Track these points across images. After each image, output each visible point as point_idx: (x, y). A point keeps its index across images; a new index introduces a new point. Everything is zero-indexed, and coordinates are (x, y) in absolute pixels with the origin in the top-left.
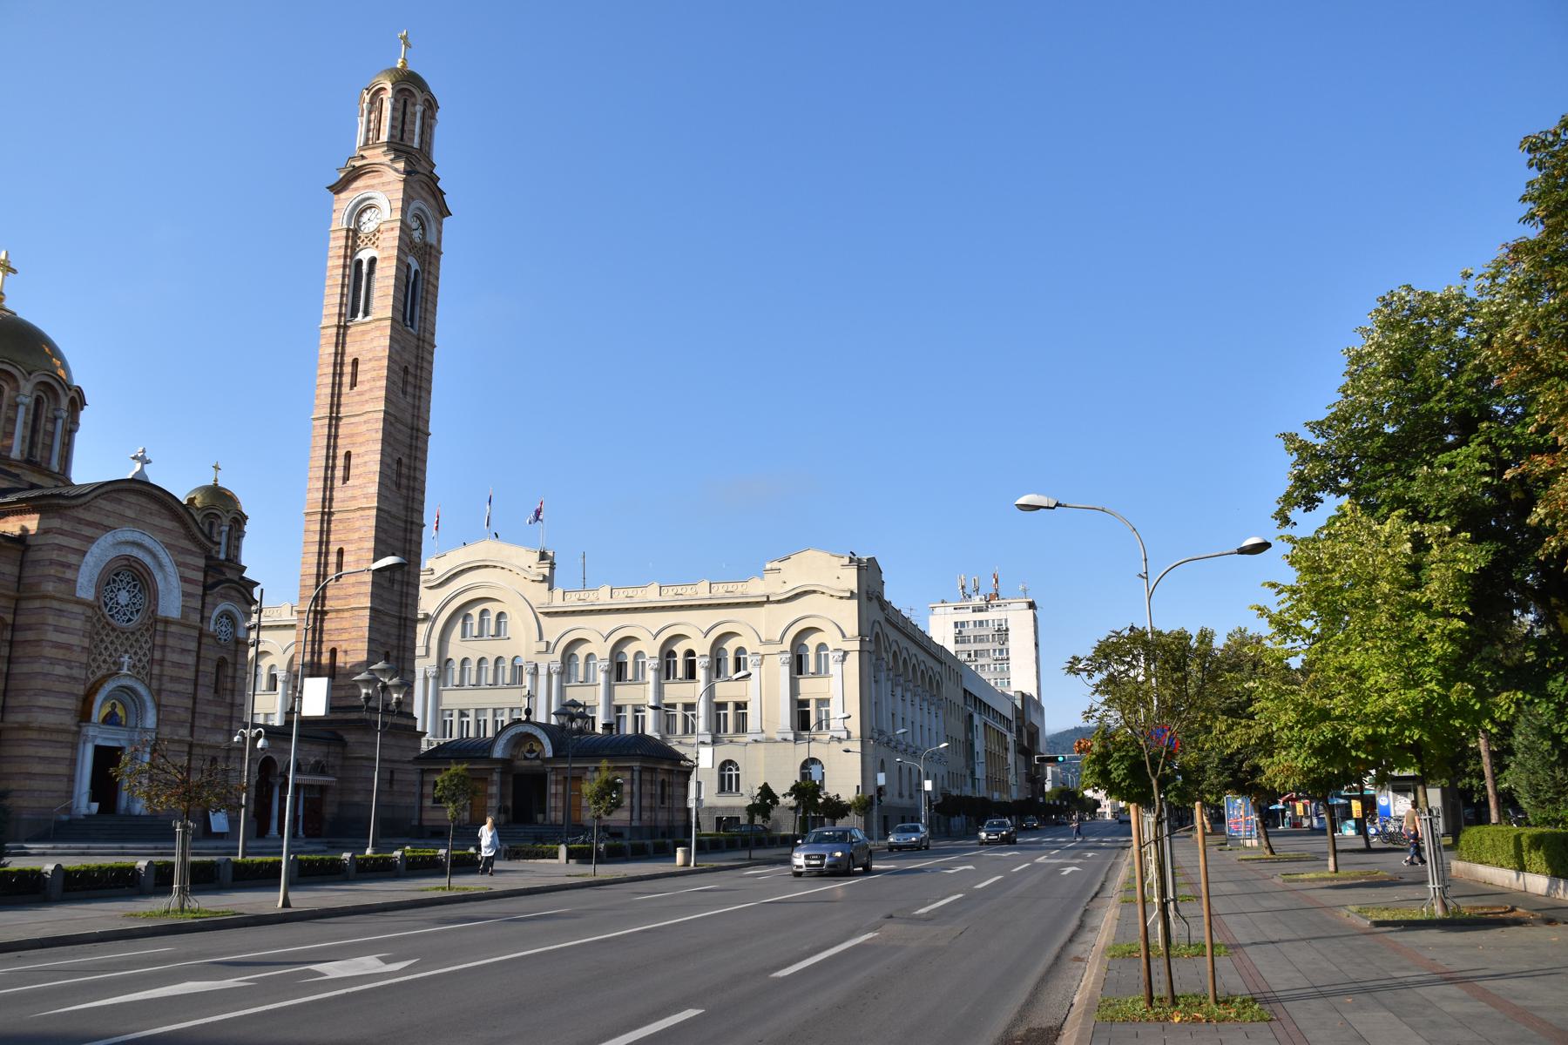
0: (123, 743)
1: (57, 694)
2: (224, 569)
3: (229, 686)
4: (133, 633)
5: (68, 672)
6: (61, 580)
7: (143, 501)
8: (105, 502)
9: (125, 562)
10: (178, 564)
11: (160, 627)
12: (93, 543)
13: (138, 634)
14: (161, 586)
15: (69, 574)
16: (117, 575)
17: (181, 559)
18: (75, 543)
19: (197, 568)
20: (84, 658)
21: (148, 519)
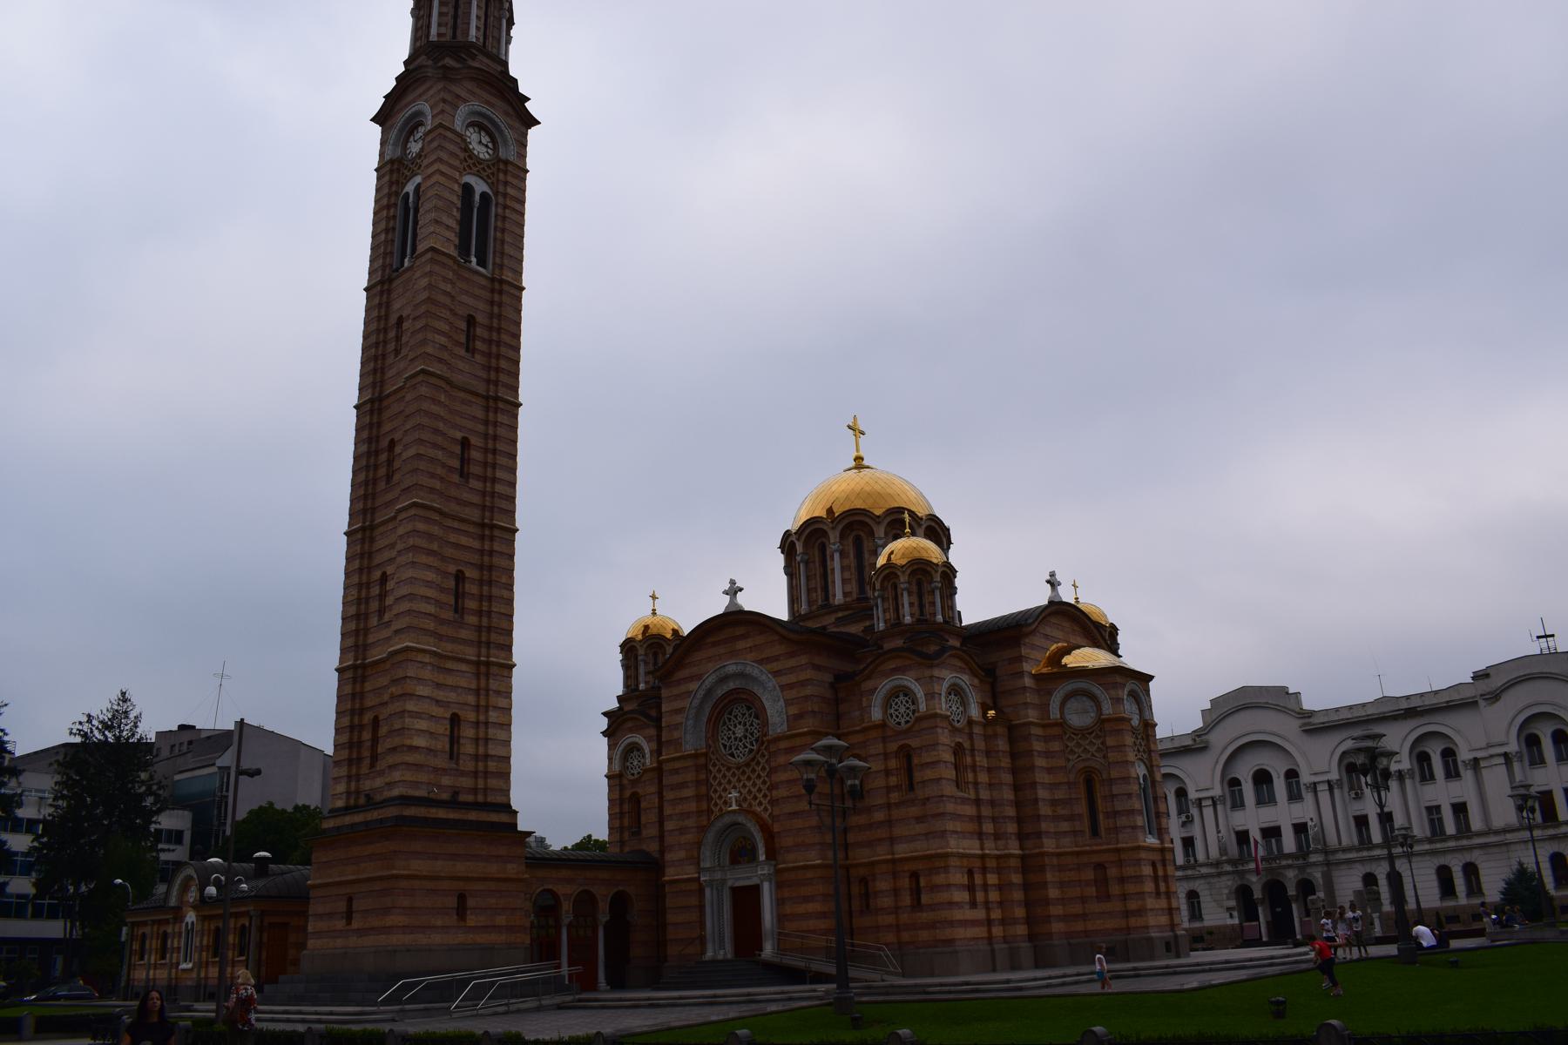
0: (755, 881)
4: (748, 765)
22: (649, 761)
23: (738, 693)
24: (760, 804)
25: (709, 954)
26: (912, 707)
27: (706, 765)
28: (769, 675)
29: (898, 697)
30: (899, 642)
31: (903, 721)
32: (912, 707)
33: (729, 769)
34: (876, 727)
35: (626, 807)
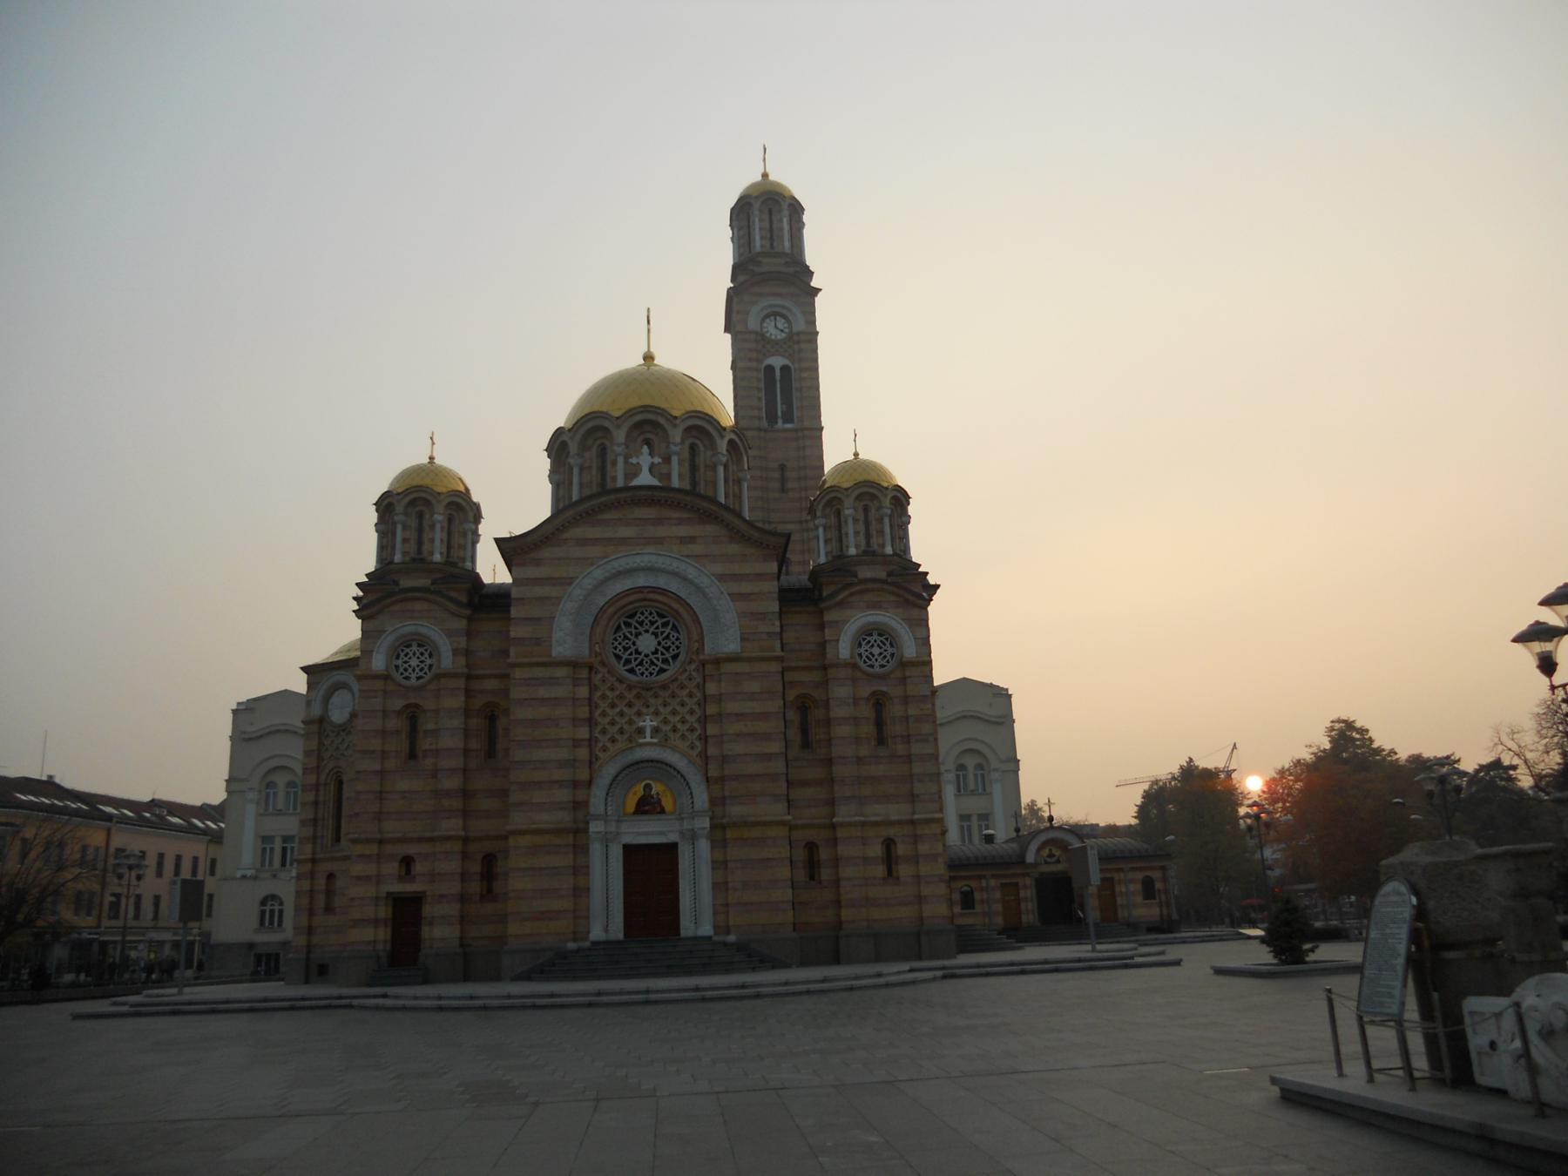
0: (672, 837)
4: (664, 687)
11: (709, 669)
12: (570, 584)
16: (632, 616)
19: (760, 577)
20: (583, 733)
21: (661, 531)
22: (447, 661)
23: (649, 592)
24: (683, 737)
25: (597, 933)
26: (890, 650)
27: (590, 679)
28: (713, 578)
29: (871, 635)
30: (880, 573)
31: (877, 664)
32: (890, 650)
33: (630, 688)
34: (846, 665)
35: (393, 723)
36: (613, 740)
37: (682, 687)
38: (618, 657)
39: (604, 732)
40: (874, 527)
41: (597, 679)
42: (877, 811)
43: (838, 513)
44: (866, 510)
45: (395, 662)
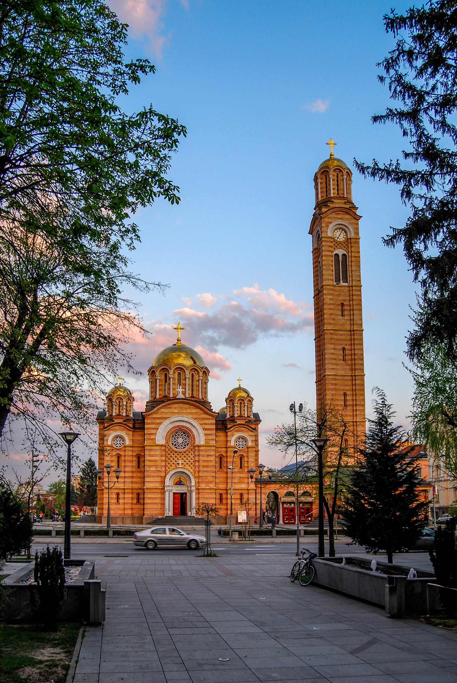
1: (153, 477)
2: (236, 421)
3: (246, 465)
4: (185, 452)
5: (157, 469)
6: (149, 439)
7: (181, 405)
8: (164, 410)
9: (179, 428)
10: (201, 424)
11: (196, 448)
13: (187, 452)
14: (195, 433)
15: (152, 437)
17: (202, 422)
18: (153, 426)
21: (185, 411)
22: (128, 442)
24: (189, 466)
33: (176, 452)
36: (171, 466)
37: (189, 452)
38: (173, 444)
39: (169, 464)
40: (242, 408)
41: (167, 450)
42: (237, 486)
43: (233, 404)
44: (241, 403)
45: (113, 442)
